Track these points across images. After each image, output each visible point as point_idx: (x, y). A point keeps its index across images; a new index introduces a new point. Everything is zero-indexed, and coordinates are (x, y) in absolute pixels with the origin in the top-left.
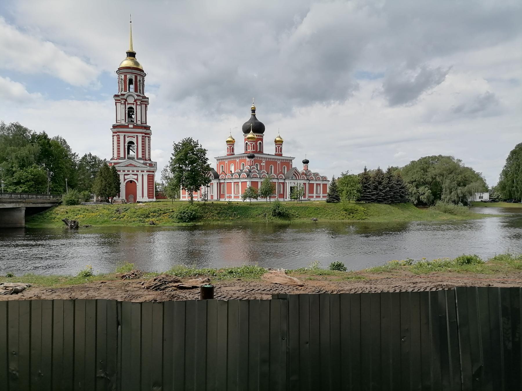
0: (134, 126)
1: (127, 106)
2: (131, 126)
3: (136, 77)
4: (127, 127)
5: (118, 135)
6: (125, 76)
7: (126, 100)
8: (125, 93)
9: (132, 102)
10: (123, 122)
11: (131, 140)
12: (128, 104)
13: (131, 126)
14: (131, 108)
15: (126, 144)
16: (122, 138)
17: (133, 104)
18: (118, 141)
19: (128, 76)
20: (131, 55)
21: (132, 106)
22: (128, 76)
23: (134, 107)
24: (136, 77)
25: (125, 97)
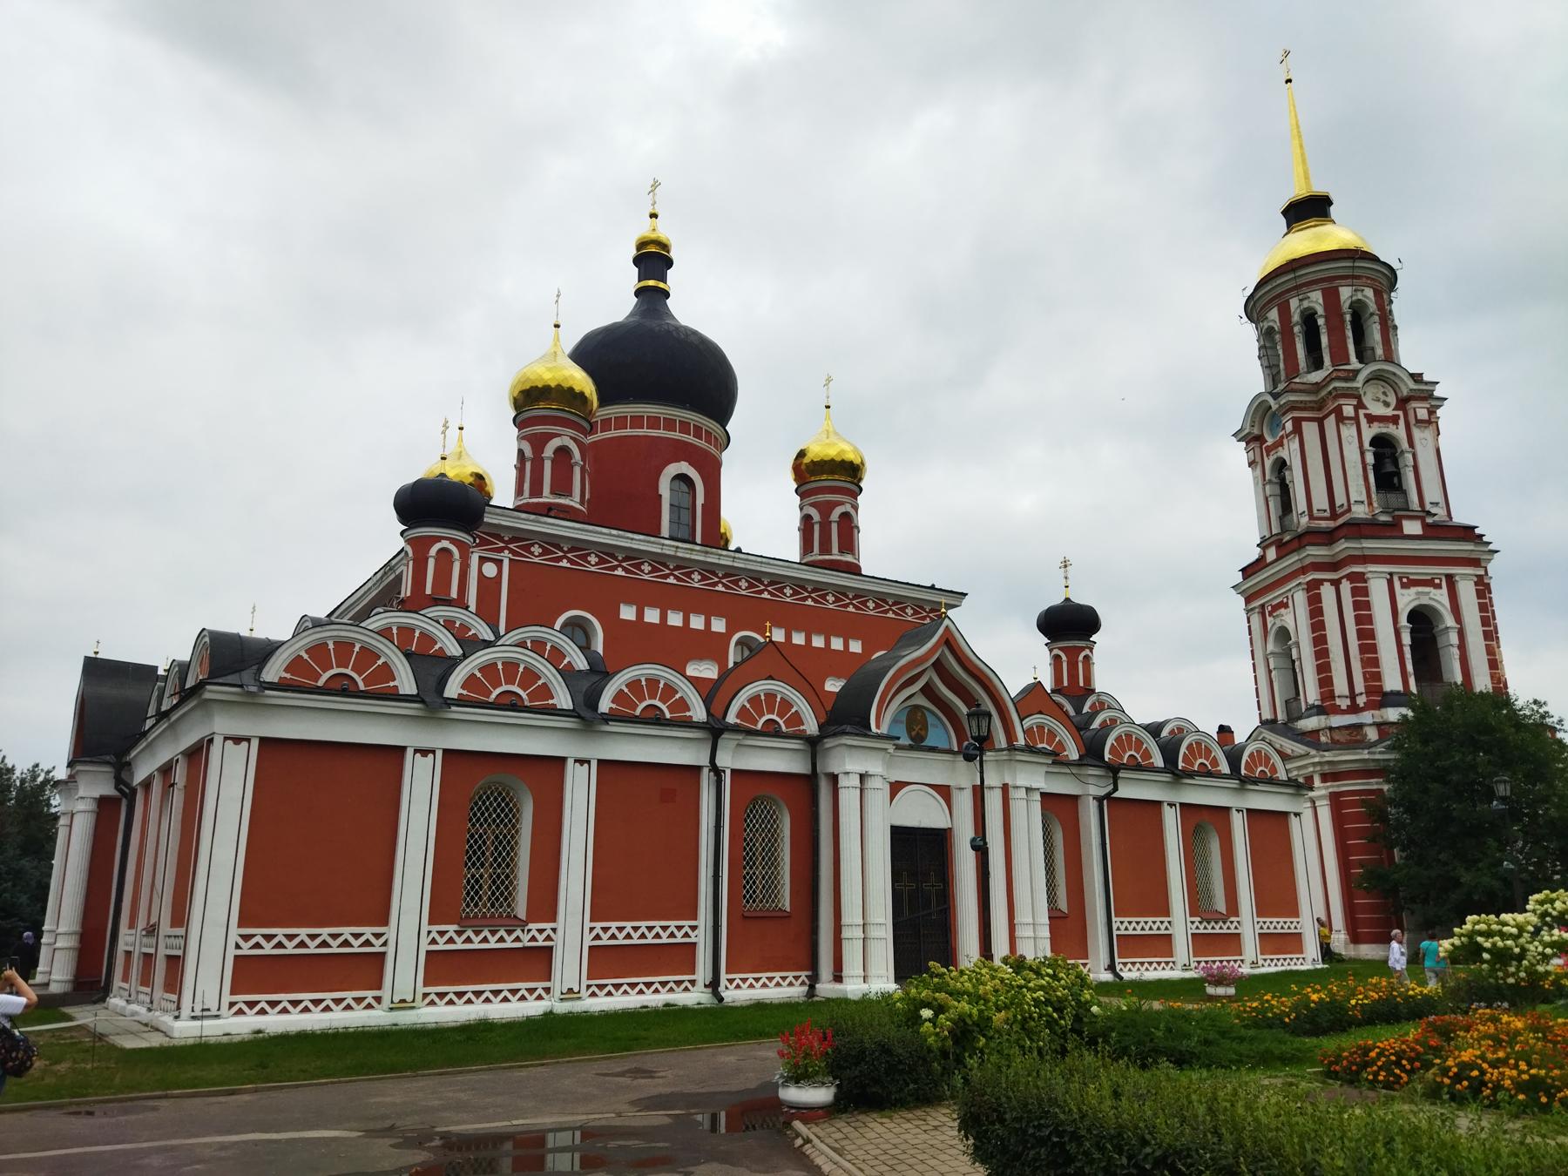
0: (1425, 526)
1: (1369, 433)
4: (1392, 529)
5: (1361, 577)
6: (1331, 297)
7: (1360, 405)
9: (1389, 412)
10: (1360, 512)
11: (1425, 601)
12: (1371, 419)
14: (1378, 441)
16: (1378, 591)
17: (1394, 420)
21: (1390, 429)
22: (1345, 293)
23: (1399, 432)
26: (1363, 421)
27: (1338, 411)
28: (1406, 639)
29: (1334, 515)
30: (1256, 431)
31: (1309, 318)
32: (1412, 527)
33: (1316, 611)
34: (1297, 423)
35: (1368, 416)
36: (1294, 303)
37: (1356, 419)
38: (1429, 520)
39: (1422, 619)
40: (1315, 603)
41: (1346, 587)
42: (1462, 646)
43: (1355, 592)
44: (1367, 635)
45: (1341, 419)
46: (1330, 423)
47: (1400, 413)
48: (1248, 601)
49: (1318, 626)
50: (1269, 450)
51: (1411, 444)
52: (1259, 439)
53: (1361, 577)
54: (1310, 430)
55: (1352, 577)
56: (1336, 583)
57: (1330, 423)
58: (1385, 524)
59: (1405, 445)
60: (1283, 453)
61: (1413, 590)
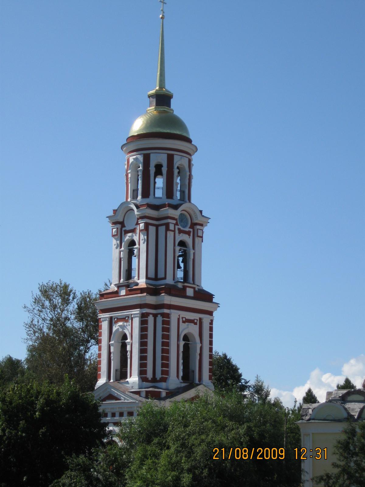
0: (195, 292)
4: (181, 293)
6: (170, 159)
9: (187, 229)
10: (169, 280)
13: (190, 292)
15: (182, 343)
17: (188, 233)
18: (166, 330)
20: (163, 99)
22: (178, 161)
26: (177, 231)
27: (167, 225)
28: (181, 349)
29: (156, 278)
30: (121, 220)
31: (159, 167)
32: (190, 292)
33: (143, 329)
34: (147, 225)
35: (179, 229)
36: (152, 157)
37: (174, 231)
39: (186, 338)
40: (143, 323)
41: (160, 319)
42: (201, 355)
43: (164, 322)
44: (166, 344)
45: (167, 229)
46: (162, 229)
47: (191, 230)
49: (143, 337)
50: (127, 232)
51: (194, 248)
52: (122, 224)
53: (168, 316)
54: (152, 229)
55: (163, 315)
56: (155, 316)
57: (162, 229)
58: (179, 290)
60: (136, 238)
61: (187, 323)
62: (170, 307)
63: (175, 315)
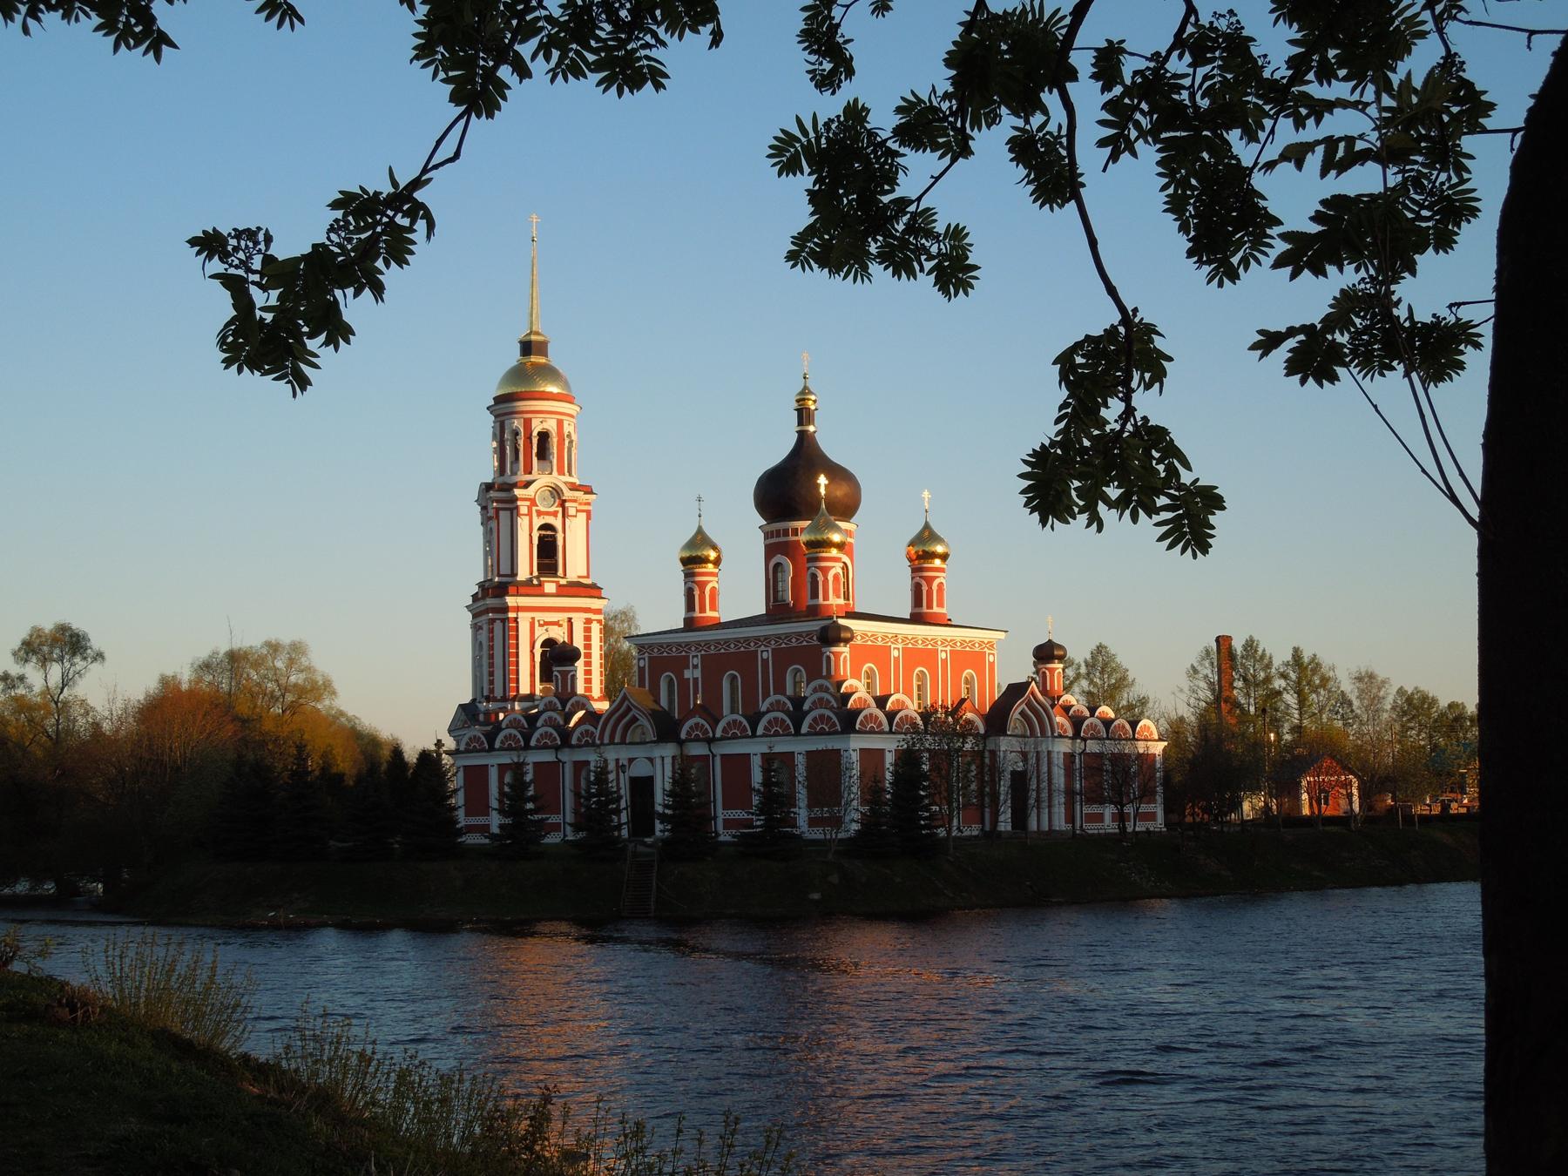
0: (559, 586)
2: (550, 587)
3: (560, 424)
6: (528, 423)
8: (528, 477)
12: (539, 513)
15: (538, 651)
17: (555, 514)
19: (537, 427)
21: (550, 520)
22: (537, 427)
24: (560, 424)
25: (530, 492)
28: (538, 659)
32: (550, 587)
37: (530, 514)
38: (563, 582)
48: (474, 616)
59: (559, 528)
62: (518, 609)
63: (524, 620)
